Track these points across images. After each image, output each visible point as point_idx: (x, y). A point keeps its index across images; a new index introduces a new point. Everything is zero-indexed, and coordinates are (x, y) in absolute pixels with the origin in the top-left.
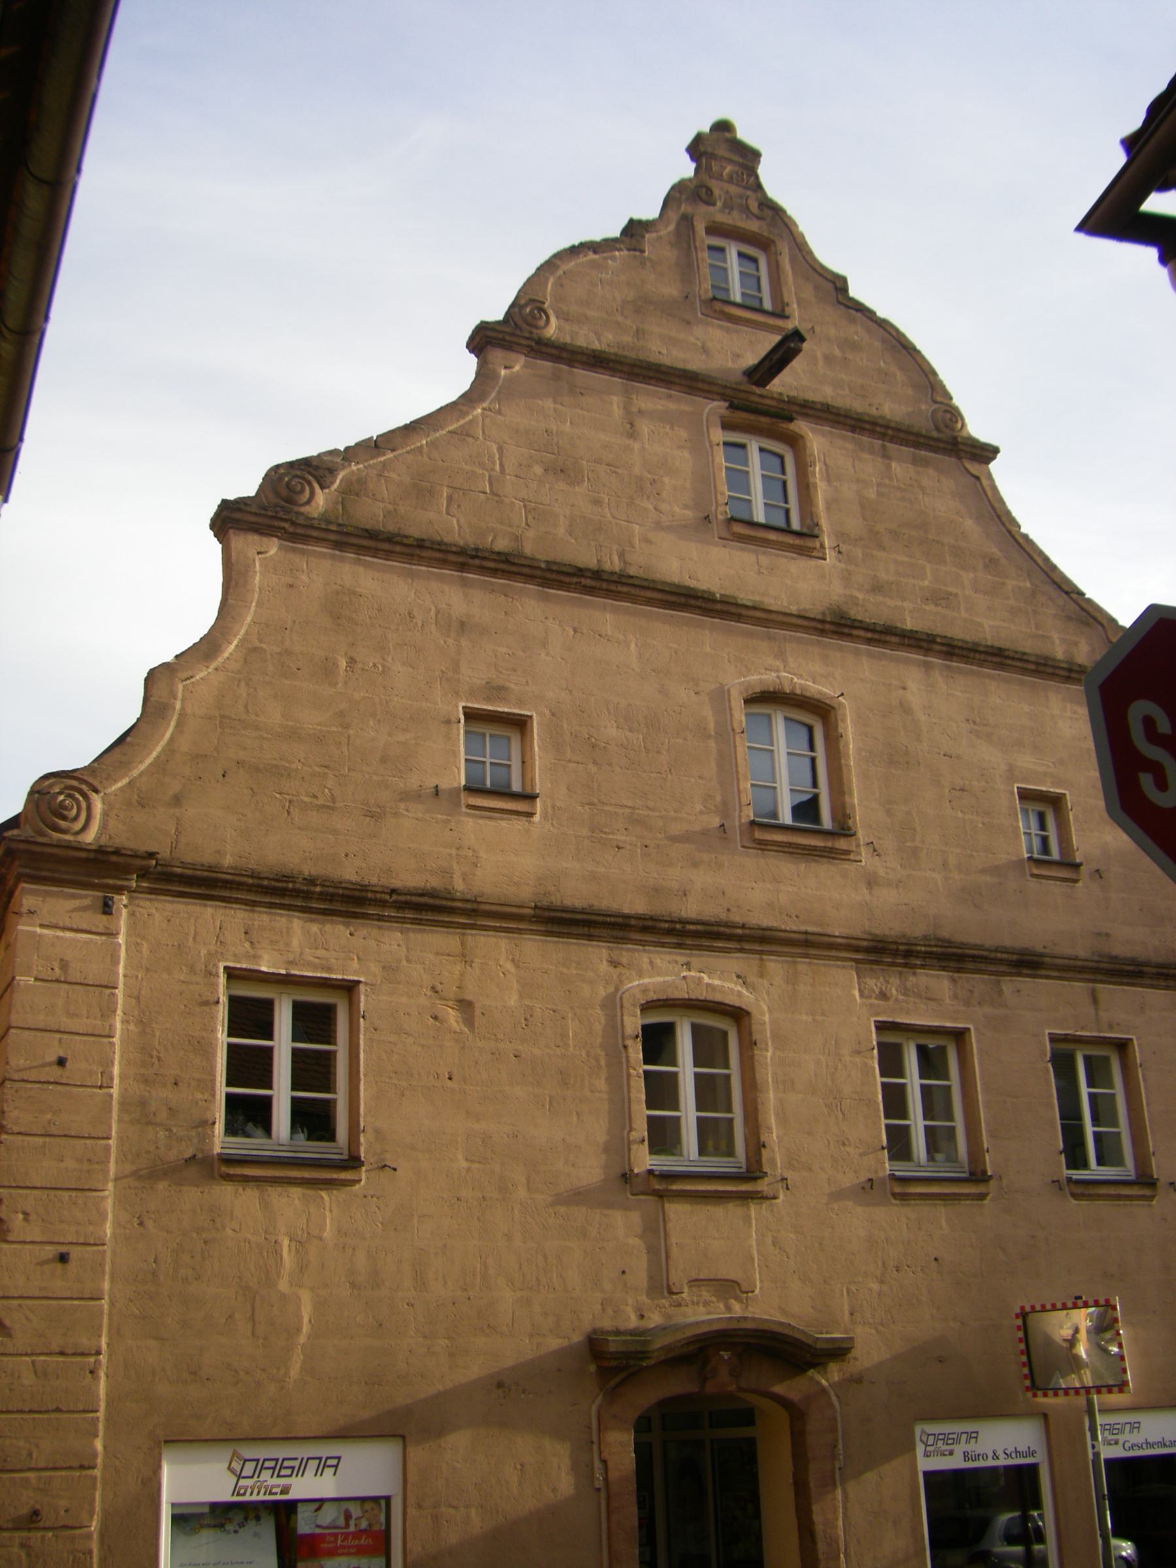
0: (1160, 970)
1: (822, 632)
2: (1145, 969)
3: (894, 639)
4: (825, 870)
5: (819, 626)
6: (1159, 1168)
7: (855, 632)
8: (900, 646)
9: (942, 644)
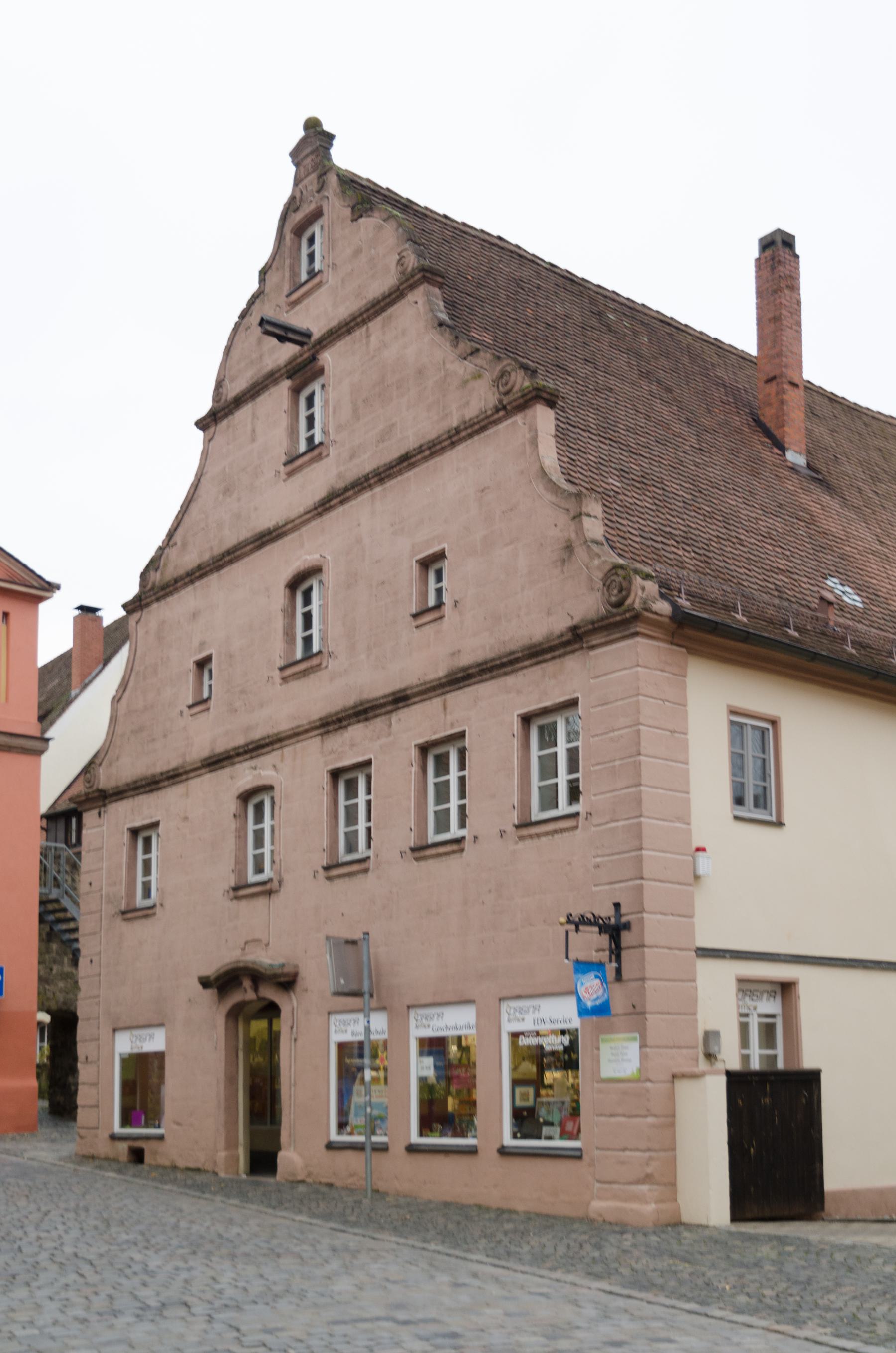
0: (481, 668)
1: (320, 515)
2: (471, 671)
3: (351, 493)
4: (312, 680)
5: (315, 512)
6: (786, 819)
7: (332, 503)
8: (357, 494)
9: (373, 477)
